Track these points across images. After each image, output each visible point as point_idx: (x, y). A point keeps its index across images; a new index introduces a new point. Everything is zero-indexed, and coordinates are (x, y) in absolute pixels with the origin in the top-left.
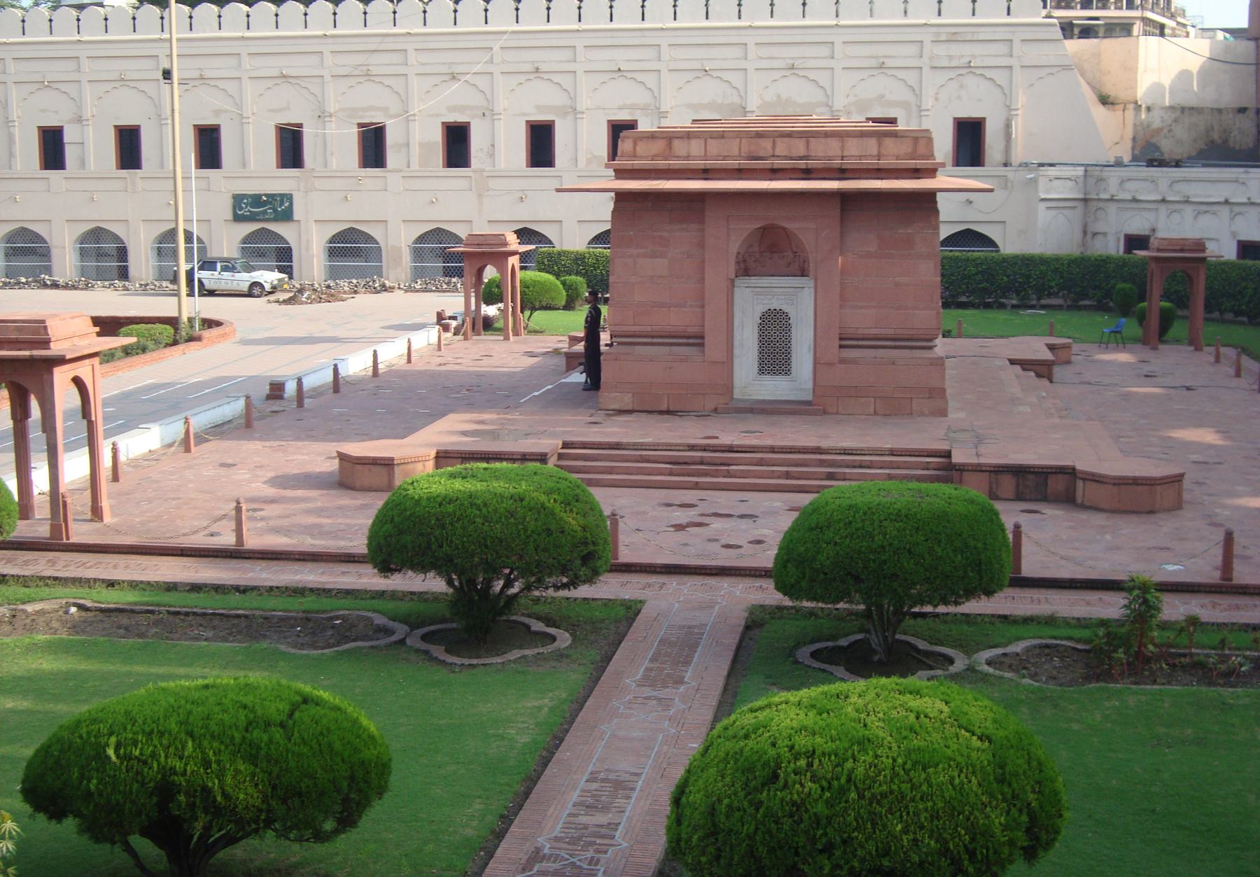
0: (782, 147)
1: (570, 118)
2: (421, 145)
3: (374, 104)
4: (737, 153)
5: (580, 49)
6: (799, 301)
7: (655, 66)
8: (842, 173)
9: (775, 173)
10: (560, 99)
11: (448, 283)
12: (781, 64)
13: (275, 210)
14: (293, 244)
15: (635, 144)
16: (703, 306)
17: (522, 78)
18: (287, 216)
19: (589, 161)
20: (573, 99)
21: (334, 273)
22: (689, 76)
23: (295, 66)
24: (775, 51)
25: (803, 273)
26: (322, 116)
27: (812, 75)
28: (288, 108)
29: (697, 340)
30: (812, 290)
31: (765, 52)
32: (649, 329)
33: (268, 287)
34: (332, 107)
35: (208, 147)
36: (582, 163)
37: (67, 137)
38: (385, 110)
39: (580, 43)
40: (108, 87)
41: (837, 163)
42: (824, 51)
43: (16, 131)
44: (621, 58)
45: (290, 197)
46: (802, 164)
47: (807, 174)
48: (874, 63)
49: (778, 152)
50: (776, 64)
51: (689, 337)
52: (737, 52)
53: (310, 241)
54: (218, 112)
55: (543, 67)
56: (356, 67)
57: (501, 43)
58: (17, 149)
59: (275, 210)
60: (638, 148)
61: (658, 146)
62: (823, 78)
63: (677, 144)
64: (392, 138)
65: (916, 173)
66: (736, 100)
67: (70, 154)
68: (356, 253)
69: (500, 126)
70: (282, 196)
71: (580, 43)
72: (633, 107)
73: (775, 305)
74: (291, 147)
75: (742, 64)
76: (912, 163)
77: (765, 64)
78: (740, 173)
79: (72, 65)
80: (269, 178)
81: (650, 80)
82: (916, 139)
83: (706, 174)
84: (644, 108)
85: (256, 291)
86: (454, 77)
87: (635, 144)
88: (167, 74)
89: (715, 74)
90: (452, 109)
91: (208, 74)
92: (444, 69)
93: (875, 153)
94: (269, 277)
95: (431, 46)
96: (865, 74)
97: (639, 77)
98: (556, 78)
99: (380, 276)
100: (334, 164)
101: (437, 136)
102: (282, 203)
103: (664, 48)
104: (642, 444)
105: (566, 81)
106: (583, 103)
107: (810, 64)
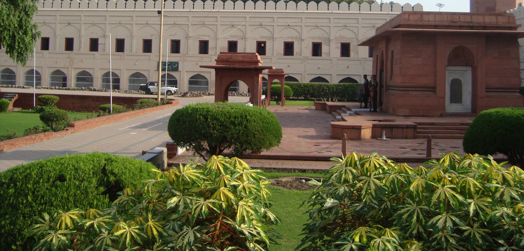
0: (462, 19)
1: (271, 40)
2: (220, 48)
3: (205, 34)
4: (446, 20)
5: (275, 18)
6: (465, 76)
7: (300, 24)
8: (485, 28)
9: (460, 27)
10: (268, 34)
11: (232, 93)
12: (341, 25)
13: (172, 67)
14: (178, 79)
15: (409, 16)
16: (436, 76)
17: (256, 27)
18: (176, 69)
19: (277, 55)
20: (273, 34)
21: (190, 89)
22: (312, 28)
23: (179, 21)
24: (341, 21)
25: (467, 65)
26: (187, 37)
27: (351, 29)
28: (176, 34)
29: (433, 89)
30: (471, 72)
31: (336, 21)
32: (415, 84)
33: (173, 92)
34: (191, 34)
35: (147, 46)
36: (275, 54)
37: (100, 42)
38: (209, 36)
39: (275, 16)
40: (115, 26)
41: (483, 25)
42: (355, 21)
43: (83, 40)
44: (289, 21)
45: (178, 63)
46: (472, 25)
47: (472, 28)
48: (371, 25)
49: (461, 20)
50: (339, 25)
51: (428, 88)
52: (327, 21)
53: (183, 78)
54: (151, 35)
55: (263, 24)
56: (200, 22)
57: (250, 16)
58: (82, 45)
59: (172, 67)
60: (410, 17)
61: (417, 17)
62: (355, 30)
63: (424, 16)
64: (210, 45)
65: (510, 28)
66: (327, 36)
67: (100, 47)
68: (196, 83)
69: (248, 43)
70: (175, 63)
71: (275, 16)
72: (292, 38)
73: (456, 77)
74: (176, 46)
75: (329, 25)
76: (510, 25)
77: (337, 25)
78: (448, 27)
79: (103, 18)
80: (169, 57)
81: (299, 29)
82: (509, 17)
83: (436, 27)
84: (296, 38)
85: (169, 93)
86: (233, 26)
87: (409, 16)
88: (159, 12)
89: (320, 28)
90: (231, 36)
91: (149, 22)
92: (230, 23)
93: (495, 21)
94: (173, 89)
95: (226, 16)
96: (369, 29)
97: (295, 28)
98: (267, 27)
99: (208, 90)
100: (190, 53)
101: (226, 45)
102: (175, 65)
103: (303, 19)
104: (440, 123)
105: (270, 28)
106: (276, 35)
107: (351, 25)
